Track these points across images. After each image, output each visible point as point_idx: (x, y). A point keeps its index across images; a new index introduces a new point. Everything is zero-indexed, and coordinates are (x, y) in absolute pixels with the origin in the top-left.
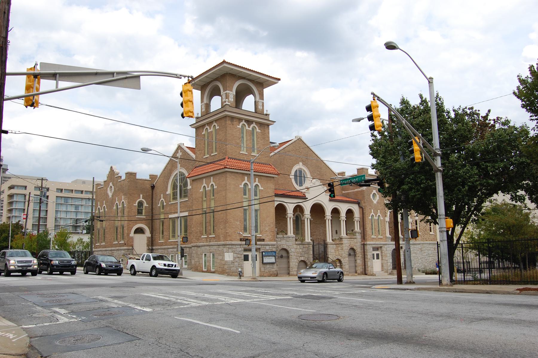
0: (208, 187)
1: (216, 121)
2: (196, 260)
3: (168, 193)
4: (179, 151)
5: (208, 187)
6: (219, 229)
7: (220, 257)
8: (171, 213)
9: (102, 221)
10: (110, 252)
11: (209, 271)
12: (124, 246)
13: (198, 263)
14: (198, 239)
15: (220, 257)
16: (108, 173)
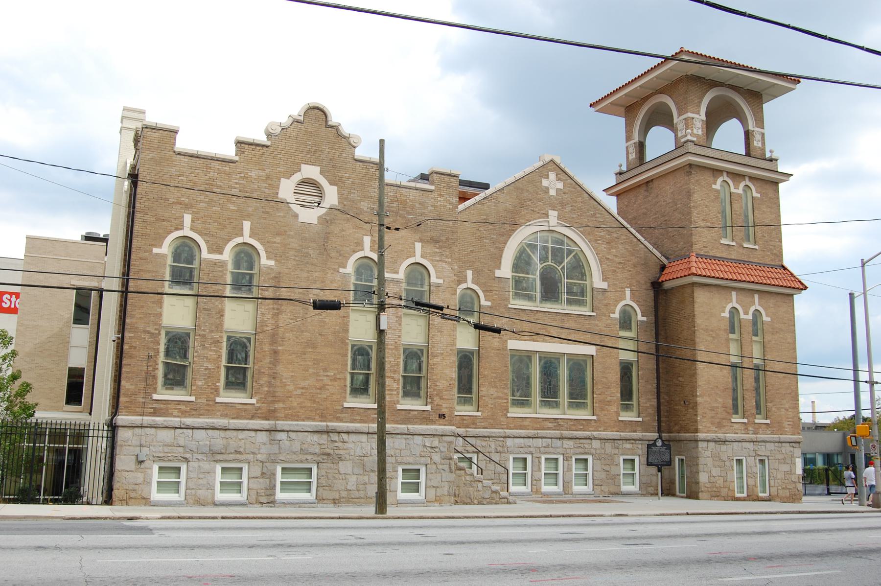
0: (746, 313)
1: (752, 178)
2: (716, 472)
3: (498, 273)
4: (552, 176)
5: (746, 313)
6: (779, 409)
7: (785, 468)
8: (518, 334)
9: (498, 331)
10: (316, 437)
11: (752, 497)
12: (433, 422)
13: (720, 482)
14: (720, 425)
15: (785, 468)
16: (285, 120)
